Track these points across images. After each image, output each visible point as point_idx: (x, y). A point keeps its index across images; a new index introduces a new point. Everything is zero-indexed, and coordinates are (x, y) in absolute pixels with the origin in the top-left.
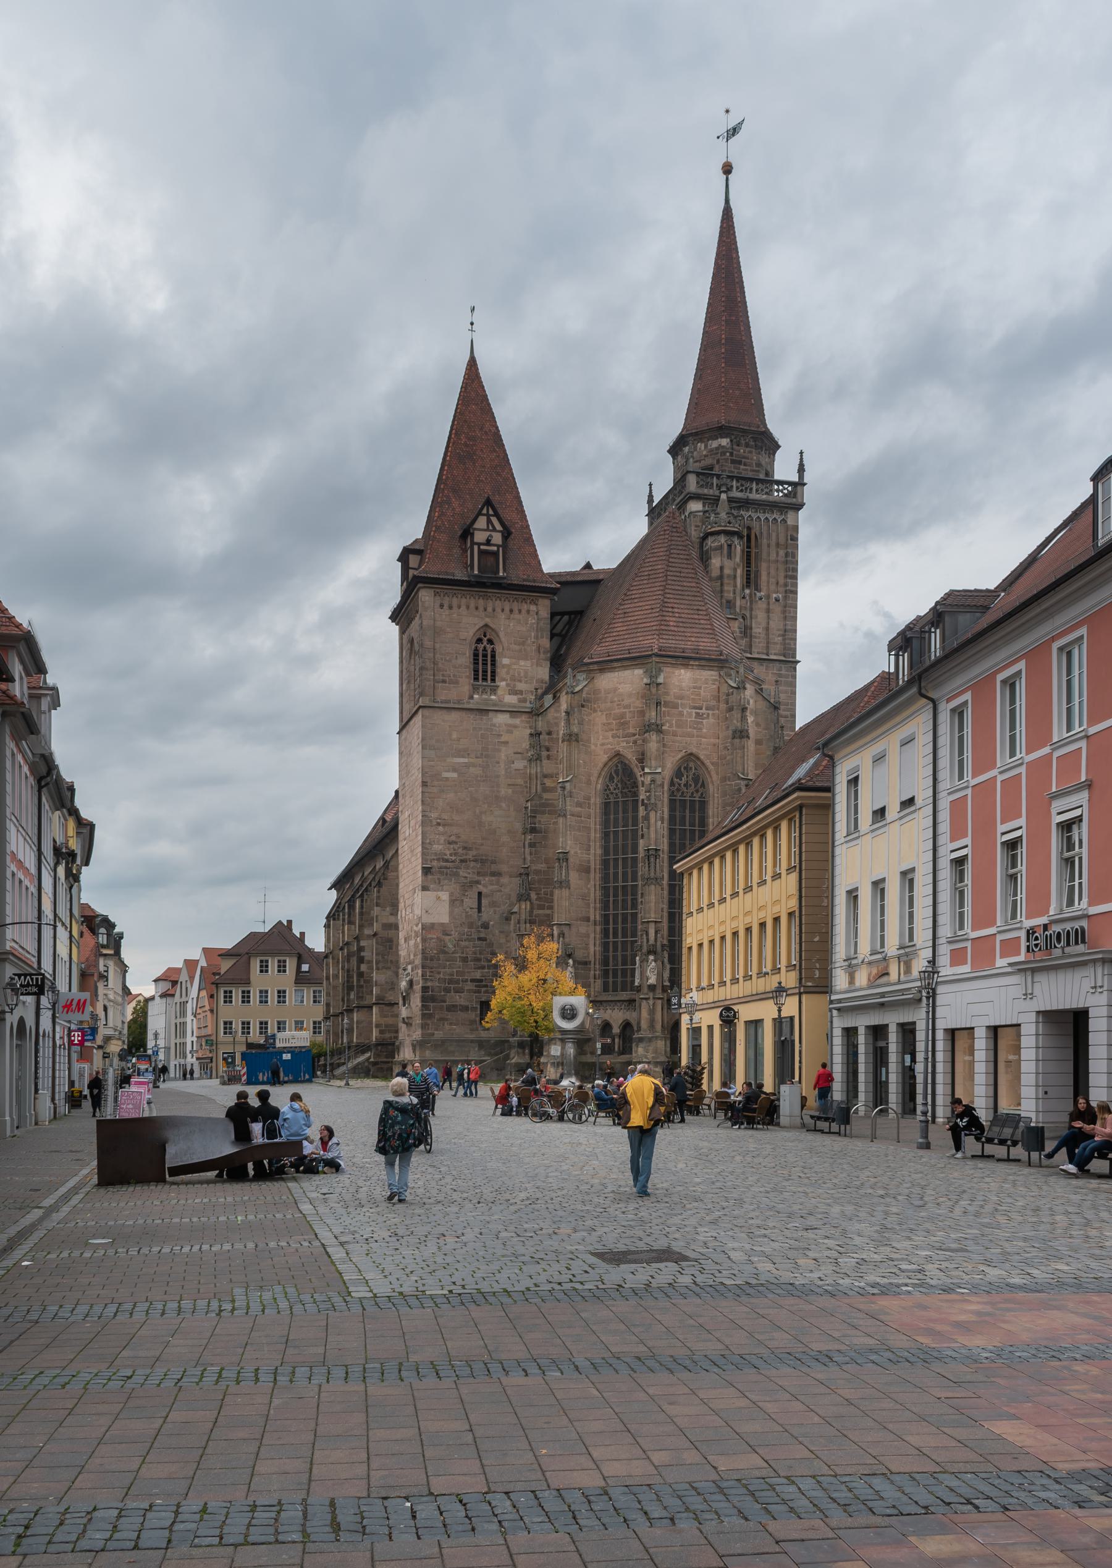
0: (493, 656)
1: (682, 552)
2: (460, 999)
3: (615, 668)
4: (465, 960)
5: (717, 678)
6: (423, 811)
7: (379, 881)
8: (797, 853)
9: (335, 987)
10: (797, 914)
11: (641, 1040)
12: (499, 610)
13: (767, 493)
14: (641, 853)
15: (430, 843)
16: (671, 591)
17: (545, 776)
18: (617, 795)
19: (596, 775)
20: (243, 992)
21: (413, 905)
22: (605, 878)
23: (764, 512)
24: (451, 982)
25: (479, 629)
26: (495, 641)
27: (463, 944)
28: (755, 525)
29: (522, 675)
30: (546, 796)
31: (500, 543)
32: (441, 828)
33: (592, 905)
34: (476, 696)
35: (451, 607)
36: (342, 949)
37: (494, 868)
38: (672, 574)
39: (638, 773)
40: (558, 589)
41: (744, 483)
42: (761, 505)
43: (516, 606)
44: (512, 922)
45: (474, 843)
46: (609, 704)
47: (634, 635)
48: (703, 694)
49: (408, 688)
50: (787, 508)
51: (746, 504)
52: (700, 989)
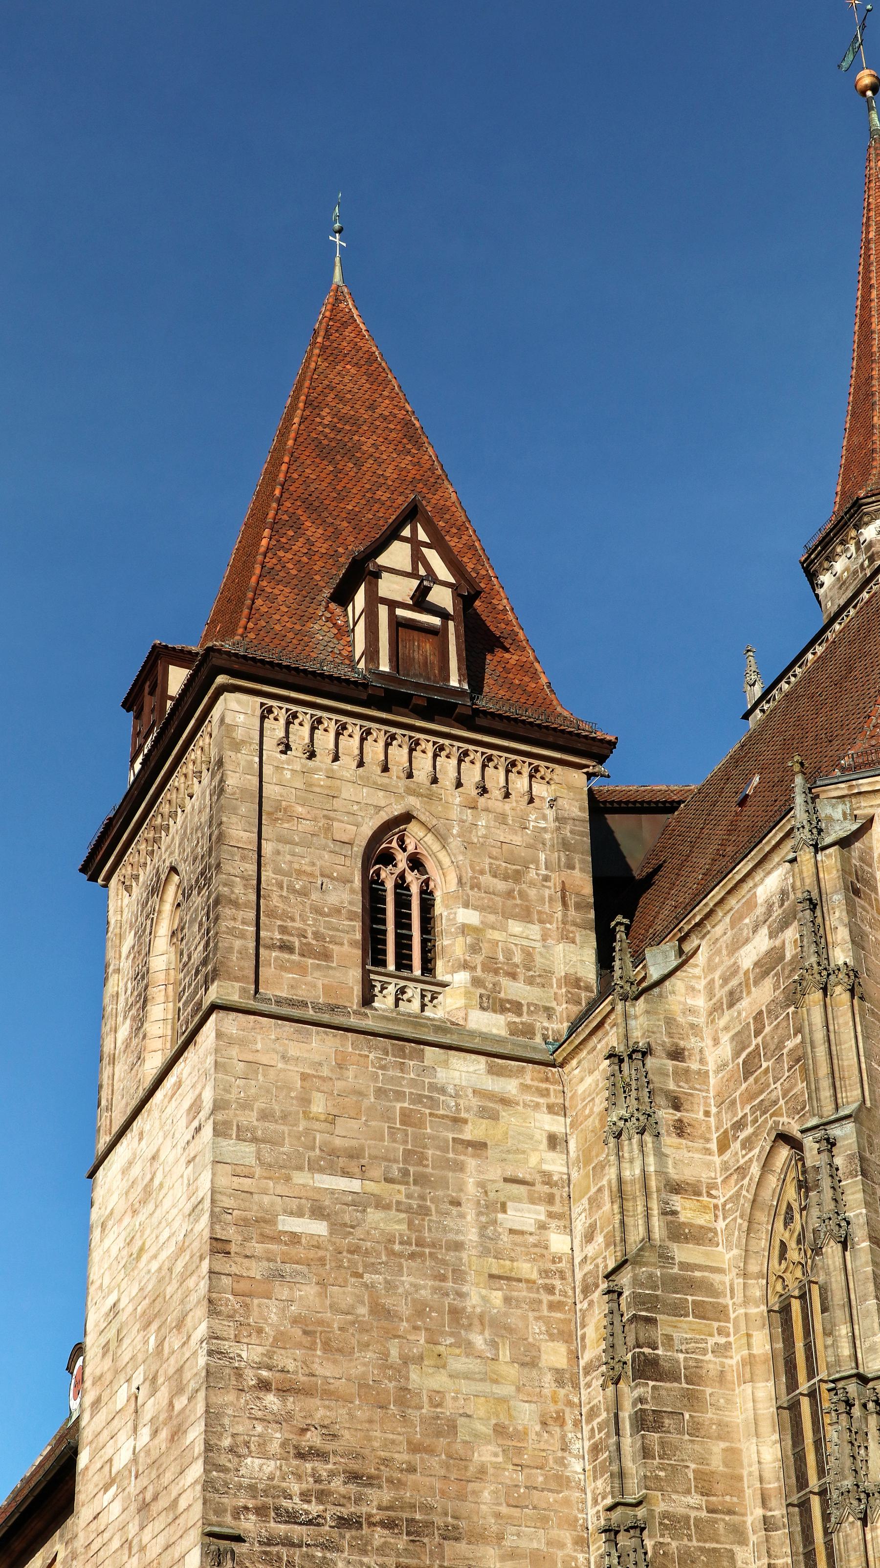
0: (427, 905)
15: (231, 1450)
26: (430, 865)
29: (517, 959)
30: (682, 1253)
32: (271, 1400)
45: (386, 1462)
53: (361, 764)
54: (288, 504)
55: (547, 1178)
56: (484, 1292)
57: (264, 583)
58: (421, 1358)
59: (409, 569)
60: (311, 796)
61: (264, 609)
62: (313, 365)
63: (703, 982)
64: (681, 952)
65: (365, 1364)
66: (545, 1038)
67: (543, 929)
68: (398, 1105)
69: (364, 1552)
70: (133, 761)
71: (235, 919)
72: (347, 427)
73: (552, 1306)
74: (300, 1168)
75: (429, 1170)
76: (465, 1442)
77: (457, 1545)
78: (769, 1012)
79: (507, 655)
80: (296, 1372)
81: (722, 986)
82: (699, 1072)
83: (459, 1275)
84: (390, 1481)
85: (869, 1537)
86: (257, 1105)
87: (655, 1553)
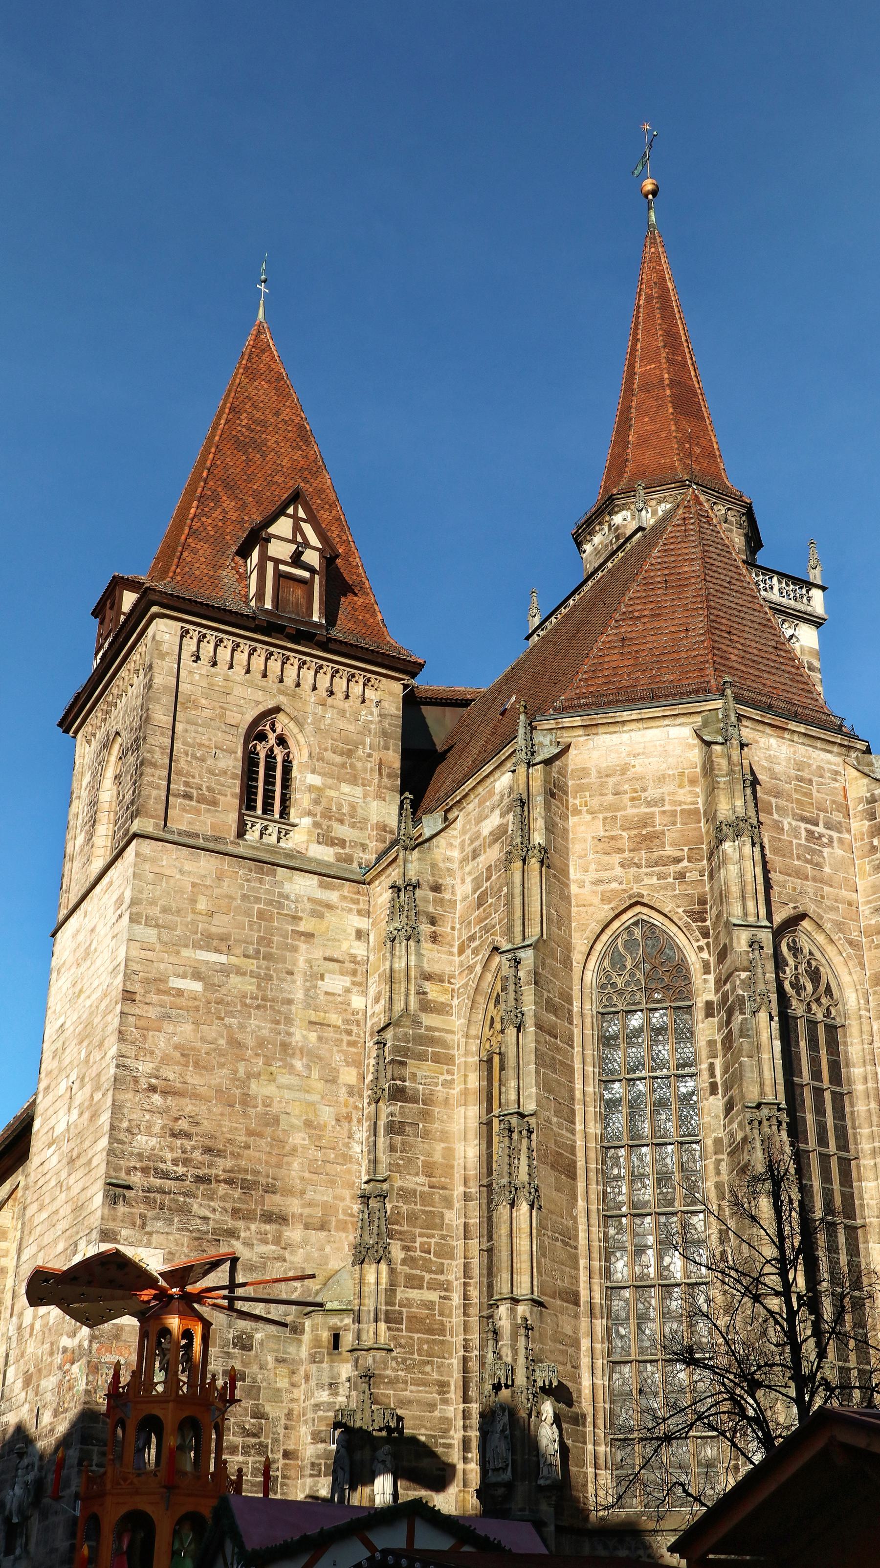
17: (428, 977)
26: (291, 742)
29: (345, 810)
30: (428, 1020)
32: (157, 1098)
33: (583, 1263)
45: (230, 1141)
53: (248, 671)
54: (212, 483)
55: (354, 959)
56: (304, 1032)
57: (190, 540)
58: (259, 1074)
59: (290, 537)
60: (212, 692)
61: (189, 559)
62: (238, 381)
63: (459, 840)
64: (446, 819)
65: (221, 1077)
66: (360, 864)
67: (365, 790)
68: (256, 906)
69: (212, 1199)
70: (96, 654)
71: (153, 776)
72: (258, 428)
73: (351, 1044)
74: (186, 946)
75: (274, 950)
76: (284, 1130)
77: (273, 1196)
78: (496, 866)
79: (356, 598)
80: (174, 1081)
81: (470, 845)
82: (450, 901)
83: (289, 1021)
84: (232, 1154)
85: (514, 1215)
87: (392, 1212)
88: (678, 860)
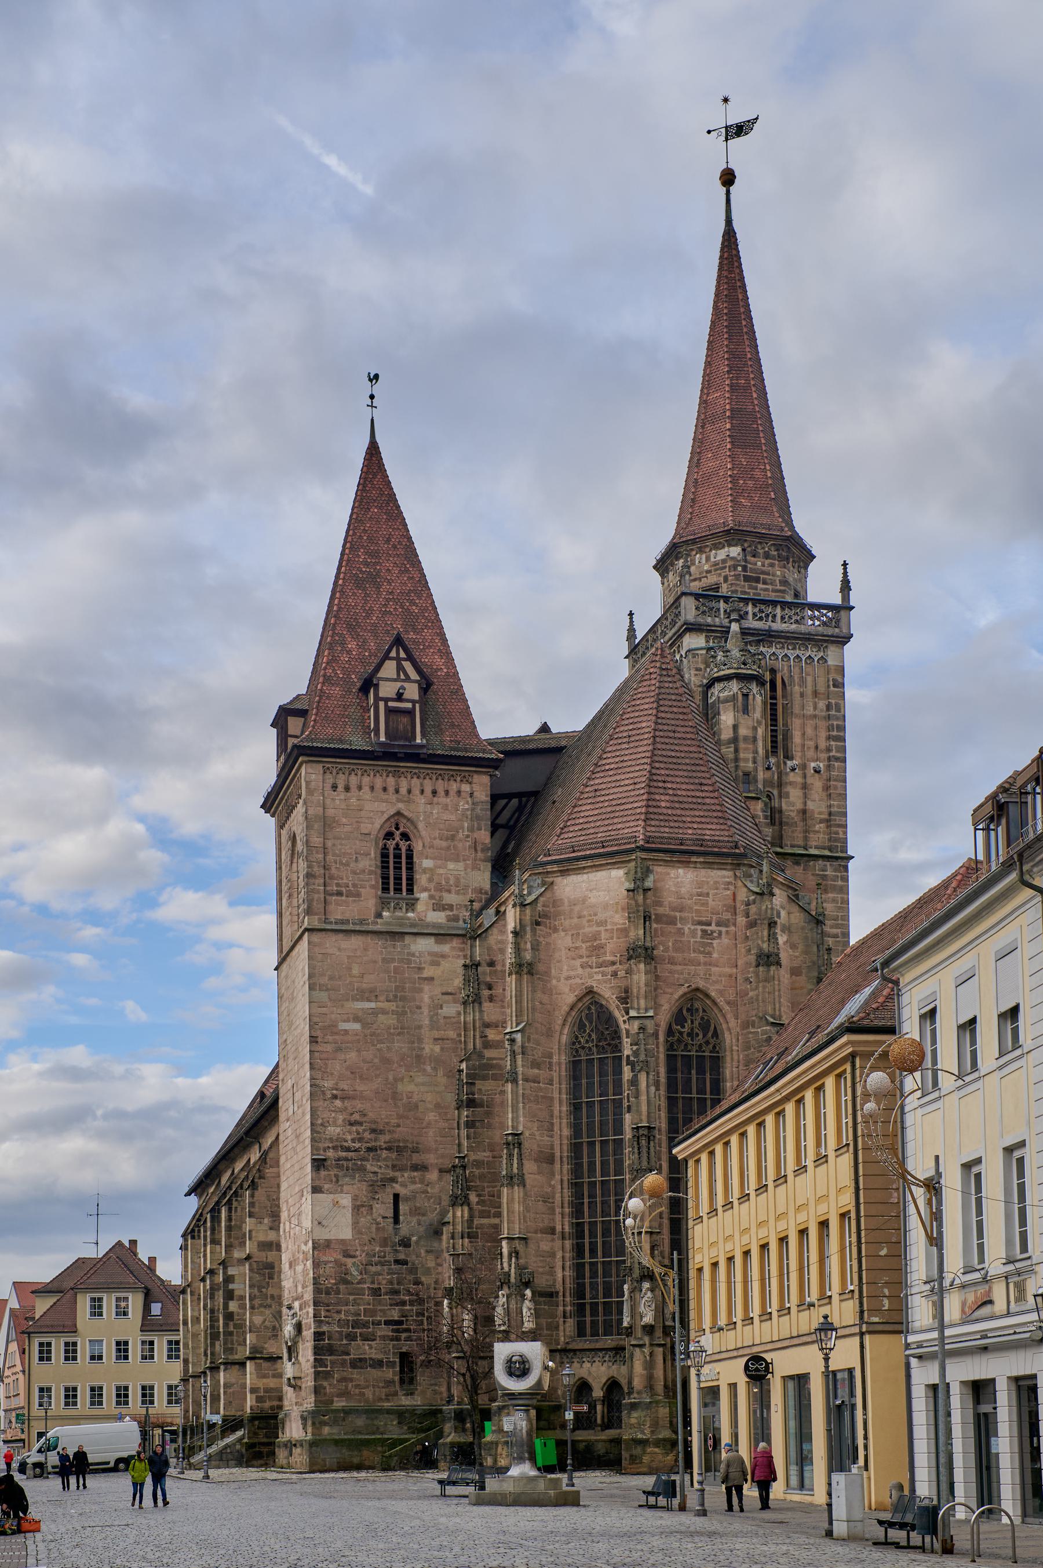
0: (410, 857)
1: (675, 704)
2: (369, 1350)
3: (584, 868)
4: (376, 1292)
5: (731, 880)
6: (312, 1078)
7: (253, 1181)
8: (850, 1124)
9: (195, 1336)
10: (853, 1215)
11: (634, 1406)
12: (416, 791)
13: (797, 622)
14: (628, 1134)
15: (322, 1125)
16: (661, 759)
17: (487, 1025)
18: (590, 1049)
19: (560, 1022)
20: (67, 1344)
21: (299, 1215)
22: (576, 1170)
23: (794, 649)
24: (356, 1324)
25: (388, 819)
26: (411, 836)
27: (373, 1269)
28: (780, 665)
29: (451, 882)
30: (489, 1053)
31: (416, 697)
32: (338, 1103)
33: (558, 1210)
34: (385, 914)
35: (347, 789)
36: (203, 1280)
37: (416, 1158)
38: (661, 734)
39: (620, 1016)
40: (500, 760)
41: (763, 607)
42: (788, 638)
43: (441, 786)
44: (444, 1237)
45: (387, 1123)
46: (576, 920)
47: (610, 821)
48: (711, 902)
49: (290, 904)
50: (826, 641)
51: (768, 637)
52: (717, 1329)
69: (378, 1161)
74: (348, 1000)
83: (420, 1040)
86: (329, 973)
88: (613, 963)
